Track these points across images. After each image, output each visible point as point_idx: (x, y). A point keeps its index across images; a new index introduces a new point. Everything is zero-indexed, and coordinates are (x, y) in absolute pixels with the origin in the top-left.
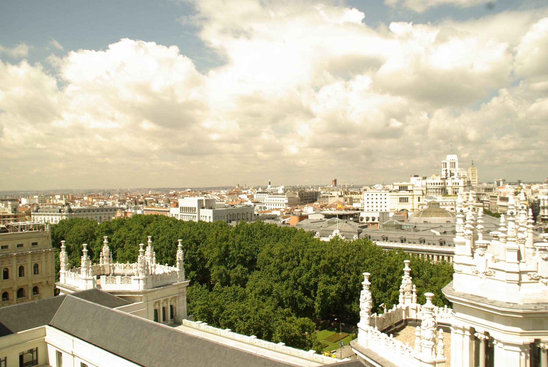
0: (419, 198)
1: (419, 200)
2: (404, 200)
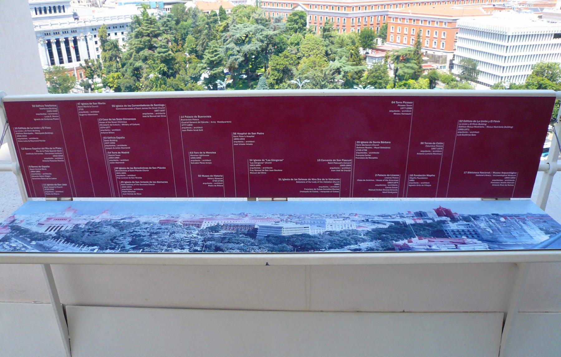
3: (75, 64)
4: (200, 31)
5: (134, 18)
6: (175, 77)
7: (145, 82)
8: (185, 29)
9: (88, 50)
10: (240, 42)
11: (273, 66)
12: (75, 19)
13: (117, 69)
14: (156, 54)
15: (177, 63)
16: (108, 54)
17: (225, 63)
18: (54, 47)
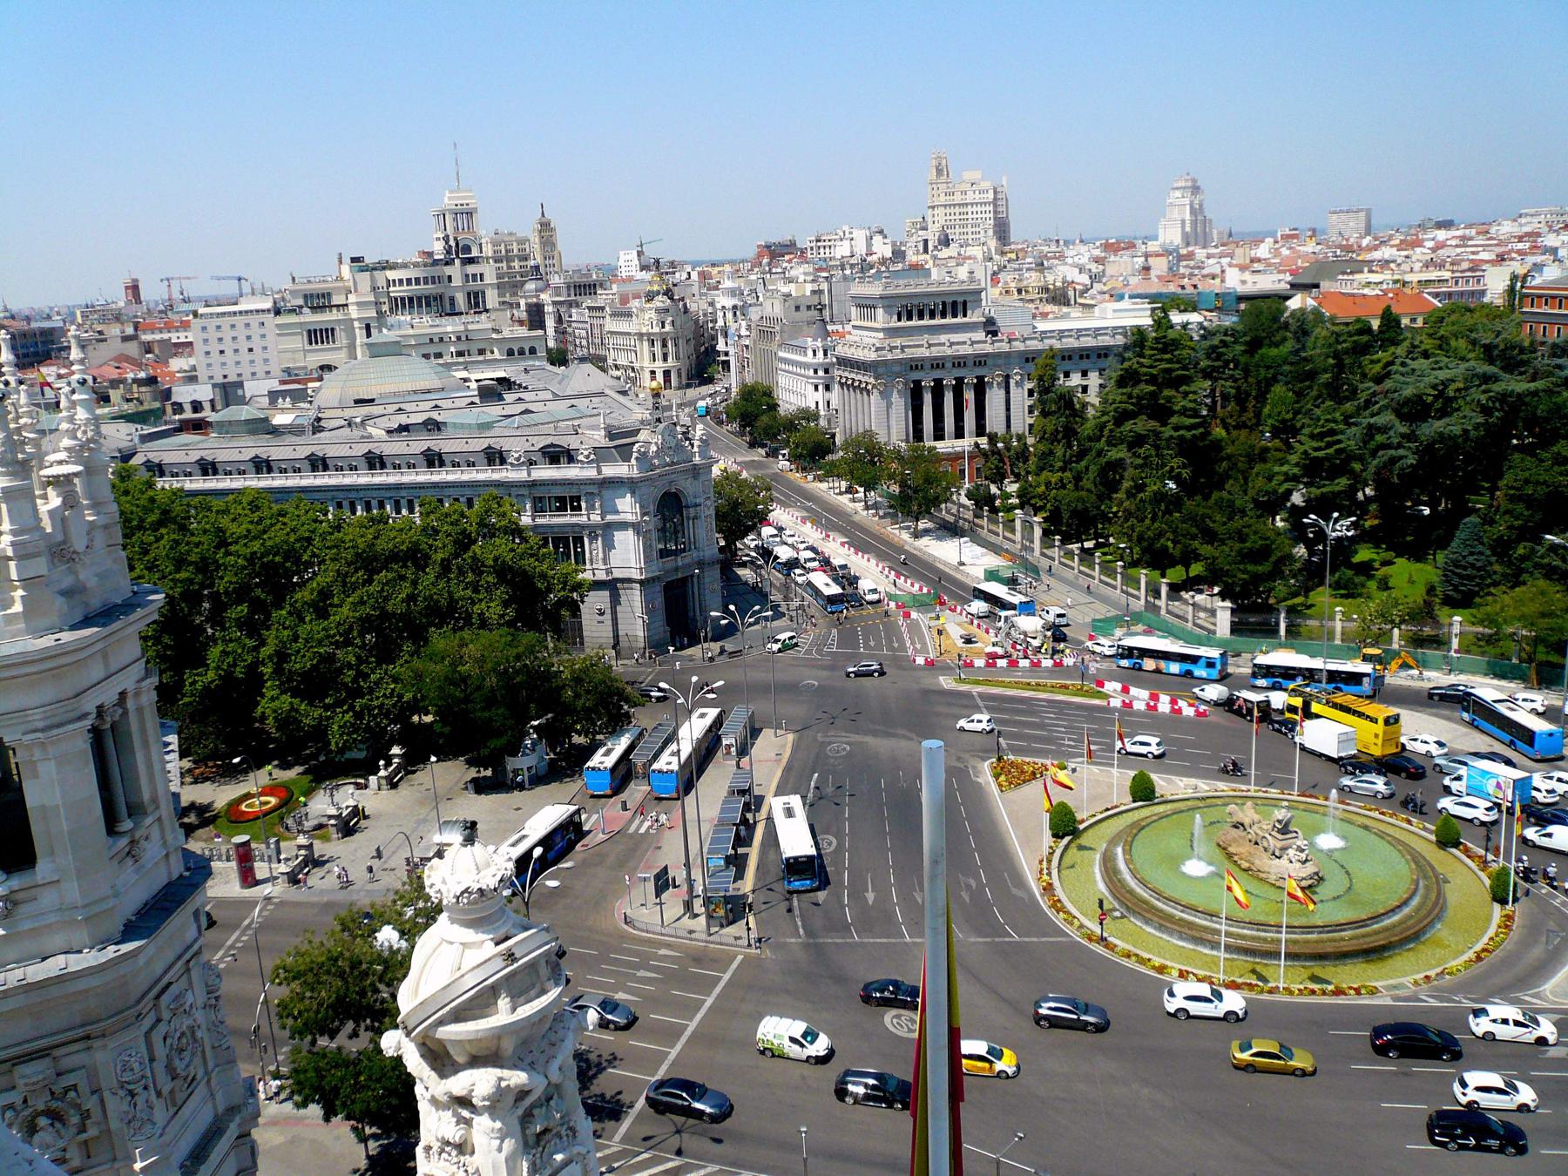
0: (368, 327)
1: (369, 335)
2: (319, 336)
3: (966, 444)
4: (1312, 375)
5: (1133, 334)
6: (1206, 497)
7: (1126, 504)
8: (1268, 368)
9: (1008, 409)
10: (1414, 410)
11: (1512, 488)
12: (988, 333)
13: (1064, 462)
14: (1167, 432)
15: (1223, 459)
16: (1051, 424)
17: (1357, 466)
18: (928, 398)
